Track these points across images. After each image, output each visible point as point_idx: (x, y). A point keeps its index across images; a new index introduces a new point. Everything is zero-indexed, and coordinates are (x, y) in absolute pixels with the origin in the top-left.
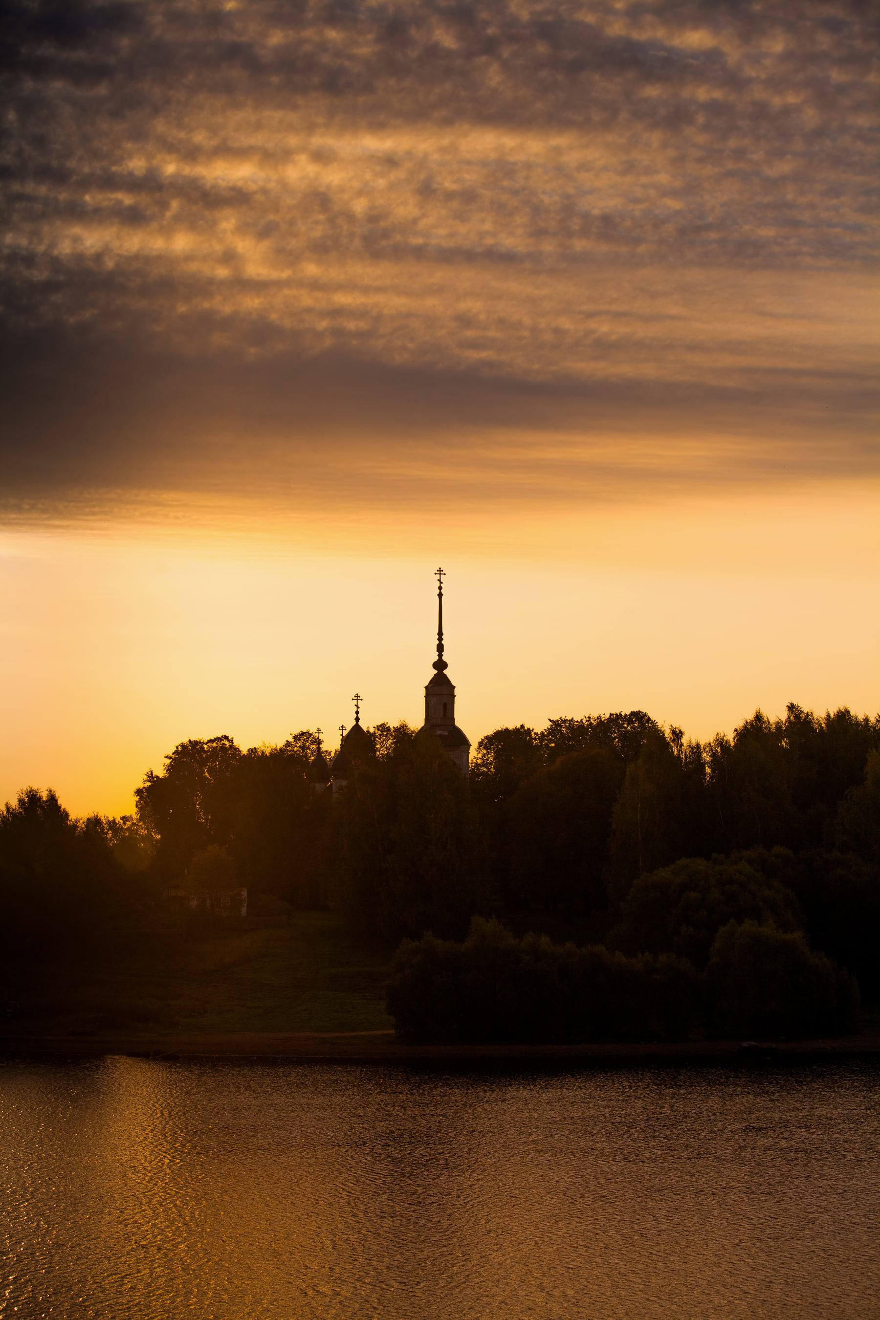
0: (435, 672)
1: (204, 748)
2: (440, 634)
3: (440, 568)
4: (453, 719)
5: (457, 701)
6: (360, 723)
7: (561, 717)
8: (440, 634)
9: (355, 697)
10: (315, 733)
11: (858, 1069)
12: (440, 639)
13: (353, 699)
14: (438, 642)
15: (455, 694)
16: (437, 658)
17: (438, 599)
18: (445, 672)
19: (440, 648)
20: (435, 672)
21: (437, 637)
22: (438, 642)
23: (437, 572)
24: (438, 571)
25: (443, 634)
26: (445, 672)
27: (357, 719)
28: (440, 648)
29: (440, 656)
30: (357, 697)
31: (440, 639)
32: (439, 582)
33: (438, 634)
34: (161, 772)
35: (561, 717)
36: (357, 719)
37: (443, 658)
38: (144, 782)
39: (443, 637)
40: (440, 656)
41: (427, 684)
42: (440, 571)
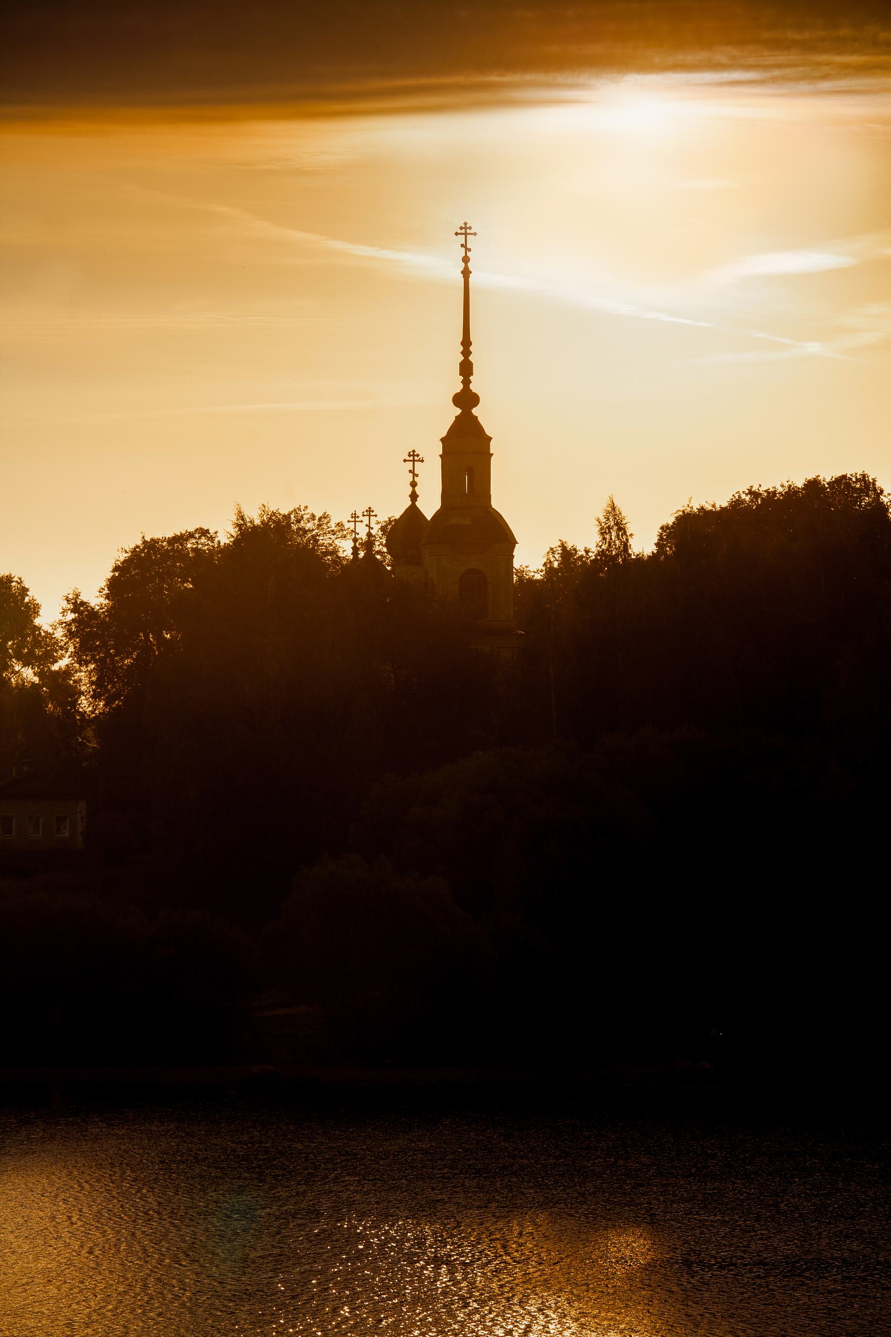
0: (458, 411)
1: (386, 540)
2: (466, 343)
3: (466, 224)
4: (488, 497)
5: (495, 465)
6: (418, 504)
7: (752, 487)
8: (466, 343)
9: (410, 455)
10: (349, 521)
11: (468, 1153)
12: (466, 353)
13: (405, 461)
14: (463, 358)
15: (491, 452)
16: (461, 386)
17: (463, 280)
18: (475, 411)
19: (466, 369)
20: (458, 411)
21: (461, 348)
22: (463, 358)
23: (459, 231)
24: (461, 228)
25: (470, 344)
26: (475, 411)
27: (414, 496)
28: (466, 369)
29: (466, 382)
30: (414, 456)
31: (466, 353)
32: (464, 249)
33: (462, 344)
34: (96, 599)
35: (752, 487)
36: (414, 496)
37: (472, 387)
38: (64, 612)
39: (471, 348)
40: (466, 382)
41: (444, 434)
42: (466, 228)
